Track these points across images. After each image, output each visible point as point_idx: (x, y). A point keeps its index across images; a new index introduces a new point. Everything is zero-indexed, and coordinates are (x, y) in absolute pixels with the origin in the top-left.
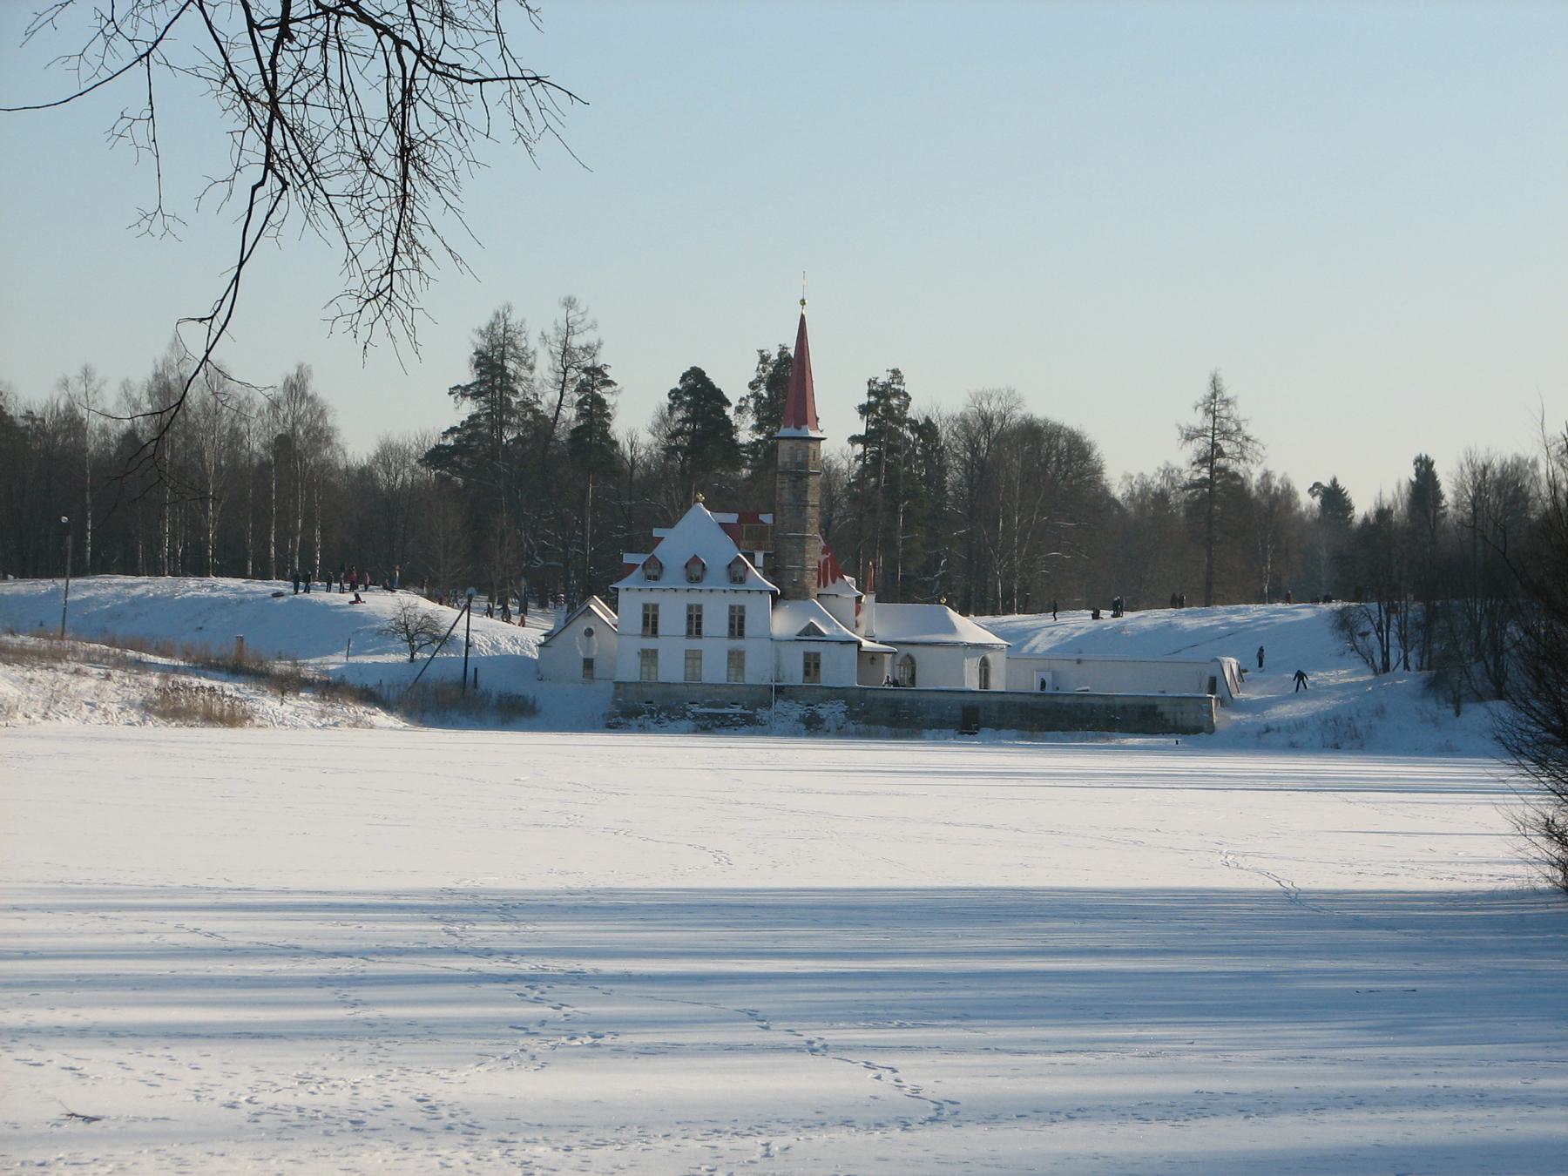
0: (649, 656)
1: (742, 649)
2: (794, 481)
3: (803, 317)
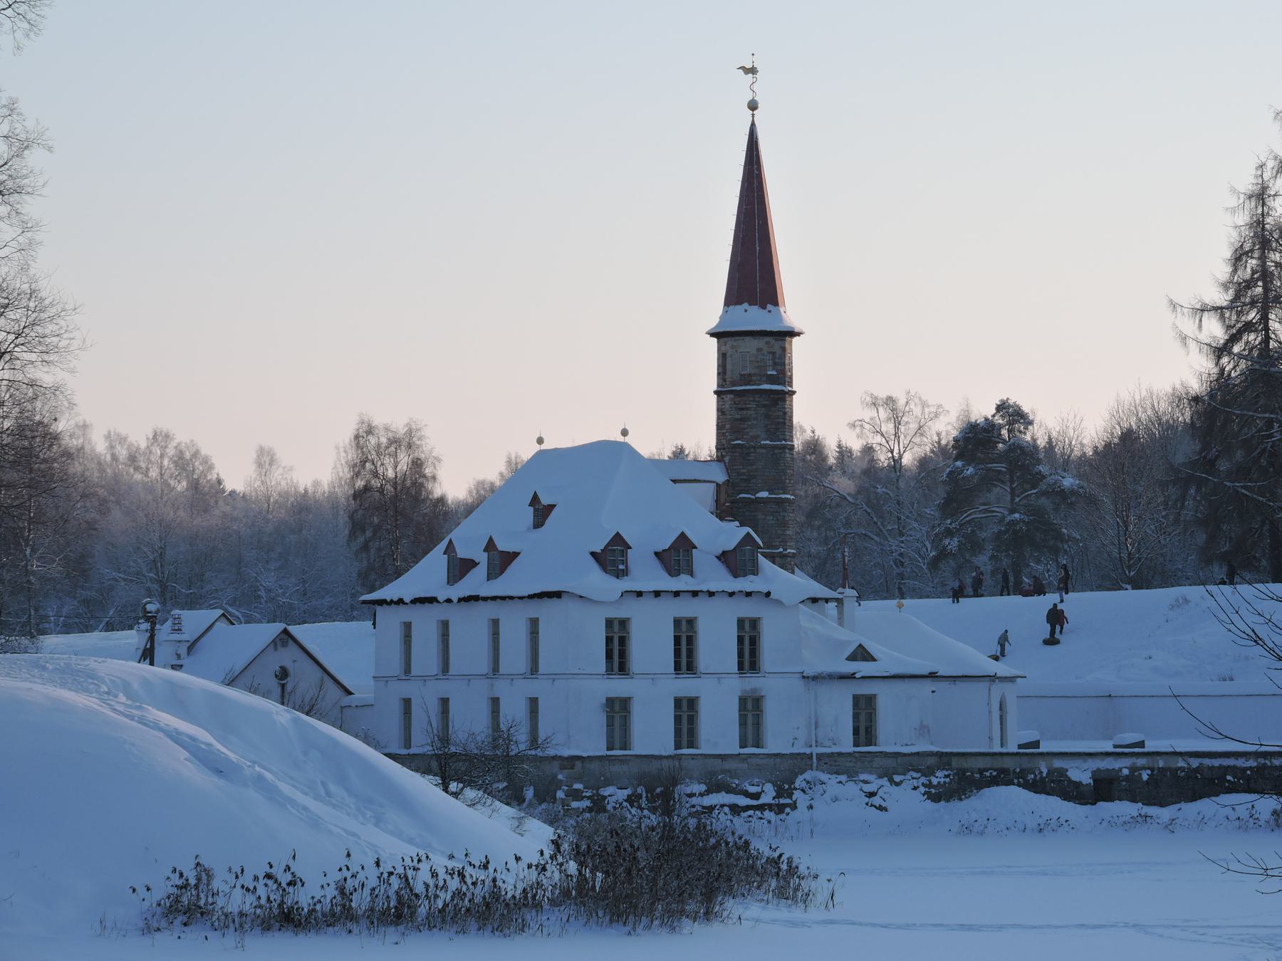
0: (618, 710)
1: (763, 694)
2: (764, 406)
3: (753, 124)
